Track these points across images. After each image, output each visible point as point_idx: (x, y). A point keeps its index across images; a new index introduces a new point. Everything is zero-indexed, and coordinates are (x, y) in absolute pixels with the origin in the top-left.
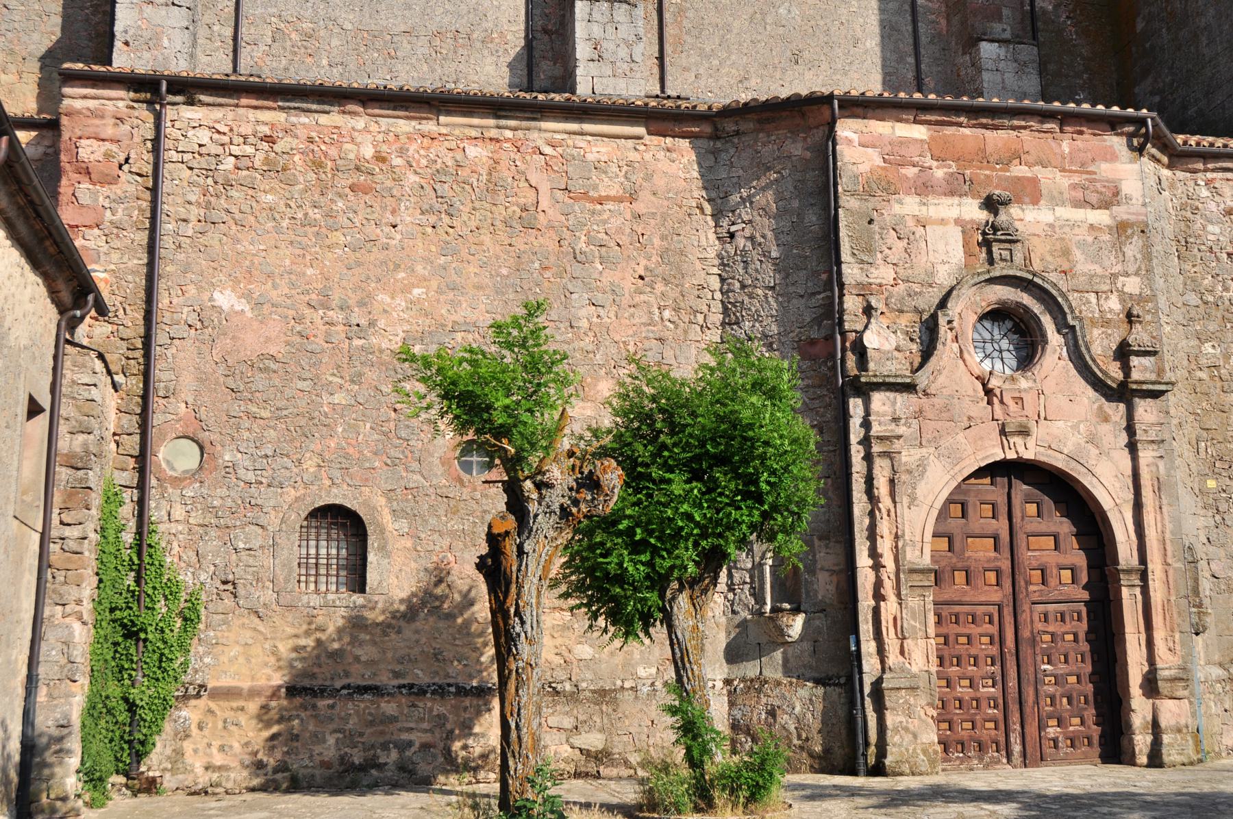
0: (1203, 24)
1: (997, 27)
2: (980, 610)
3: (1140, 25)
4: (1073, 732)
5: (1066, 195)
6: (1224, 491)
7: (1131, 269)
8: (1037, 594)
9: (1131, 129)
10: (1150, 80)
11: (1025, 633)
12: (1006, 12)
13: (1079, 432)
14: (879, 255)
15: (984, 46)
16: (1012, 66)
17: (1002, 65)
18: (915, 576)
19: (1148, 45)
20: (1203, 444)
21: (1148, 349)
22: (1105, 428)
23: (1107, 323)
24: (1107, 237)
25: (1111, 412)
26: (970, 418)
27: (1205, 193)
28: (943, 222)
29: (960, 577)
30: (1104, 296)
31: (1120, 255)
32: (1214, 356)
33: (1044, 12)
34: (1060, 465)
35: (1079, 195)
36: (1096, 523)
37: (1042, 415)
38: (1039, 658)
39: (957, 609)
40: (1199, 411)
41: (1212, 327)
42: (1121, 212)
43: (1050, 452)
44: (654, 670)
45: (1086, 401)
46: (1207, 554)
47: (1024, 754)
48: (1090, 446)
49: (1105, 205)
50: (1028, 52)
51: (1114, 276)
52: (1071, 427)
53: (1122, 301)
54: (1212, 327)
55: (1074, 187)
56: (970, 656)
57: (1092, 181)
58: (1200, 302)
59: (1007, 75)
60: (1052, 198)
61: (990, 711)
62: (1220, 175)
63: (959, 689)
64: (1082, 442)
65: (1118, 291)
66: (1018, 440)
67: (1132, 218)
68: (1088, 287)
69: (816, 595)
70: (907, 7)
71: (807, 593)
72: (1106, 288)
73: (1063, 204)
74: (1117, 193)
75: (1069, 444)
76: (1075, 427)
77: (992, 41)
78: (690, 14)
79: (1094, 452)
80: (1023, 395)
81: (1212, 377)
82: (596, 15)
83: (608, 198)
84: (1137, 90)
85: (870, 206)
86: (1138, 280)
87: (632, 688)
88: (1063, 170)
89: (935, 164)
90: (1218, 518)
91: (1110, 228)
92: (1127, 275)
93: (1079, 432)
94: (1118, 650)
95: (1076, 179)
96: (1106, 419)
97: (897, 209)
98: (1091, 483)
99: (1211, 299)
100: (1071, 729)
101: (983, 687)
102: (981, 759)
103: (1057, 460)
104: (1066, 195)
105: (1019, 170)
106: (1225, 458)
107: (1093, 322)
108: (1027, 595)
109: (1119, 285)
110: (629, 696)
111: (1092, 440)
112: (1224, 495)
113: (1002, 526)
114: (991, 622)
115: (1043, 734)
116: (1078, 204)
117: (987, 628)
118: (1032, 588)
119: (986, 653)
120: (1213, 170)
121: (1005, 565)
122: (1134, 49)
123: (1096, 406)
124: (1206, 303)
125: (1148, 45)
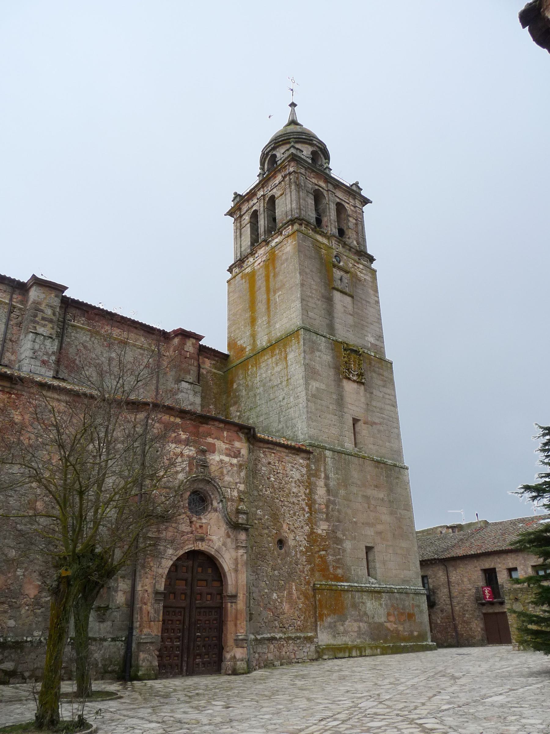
0: (258, 392)
1: (188, 377)
2: (178, 610)
3: (235, 386)
5: (224, 452)
9: (246, 431)
10: (237, 406)
11: (193, 620)
12: (192, 372)
15: (183, 383)
16: (192, 392)
17: (189, 391)
19: (237, 394)
22: (229, 540)
23: (233, 500)
24: (235, 469)
25: (231, 534)
29: (172, 596)
32: (260, 515)
33: (203, 374)
34: (213, 553)
35: (228, 452)
36: (221, 577)
39: (170, 609)
43: (209, 548)
44: (40, 633)
47: (187, 671)
48: (223, 547)
50: (198, 388)
51: (237, 483)
53: (238, 493)
54: (261, 504)
55: (227, 449)
56: (172, 629)
57: (232, 447)
59: (190, 396)
60: (219, 452)
62: (267, 450)
63: (167, 643)
64: (221, 545)
68: (228, 486)
69: (116, 601)
71: (113, 600)
72: (233, 487)
73: (223, 455)
74: (240, 453)
75: (216, 545)
76: (219, 539)
77: (186, 382)
79: (224, 549)
80: (203, 525)
81: (259, 523)
82: (37, 340)
84: (231, 409)
86: (243, 485)
87: (30, 641)
88: (224, 442)
89: (182, 433)
92: (240, 483)
94: (224, 628)
95: (227, 446)
96: (229, 536)
99: (261, 494)
100: (205, 660)
104: (224, 452)
105: (210, 440)
110: (29, 645)
111: (224, 544)
113: (189, 576)
114: (181, 615)
116: (227, 455)
117: (179, 617)
118: (197, 602)
121: (188, 592)
122: (232, 394)
124: (260, 495)
125: (237, 394)
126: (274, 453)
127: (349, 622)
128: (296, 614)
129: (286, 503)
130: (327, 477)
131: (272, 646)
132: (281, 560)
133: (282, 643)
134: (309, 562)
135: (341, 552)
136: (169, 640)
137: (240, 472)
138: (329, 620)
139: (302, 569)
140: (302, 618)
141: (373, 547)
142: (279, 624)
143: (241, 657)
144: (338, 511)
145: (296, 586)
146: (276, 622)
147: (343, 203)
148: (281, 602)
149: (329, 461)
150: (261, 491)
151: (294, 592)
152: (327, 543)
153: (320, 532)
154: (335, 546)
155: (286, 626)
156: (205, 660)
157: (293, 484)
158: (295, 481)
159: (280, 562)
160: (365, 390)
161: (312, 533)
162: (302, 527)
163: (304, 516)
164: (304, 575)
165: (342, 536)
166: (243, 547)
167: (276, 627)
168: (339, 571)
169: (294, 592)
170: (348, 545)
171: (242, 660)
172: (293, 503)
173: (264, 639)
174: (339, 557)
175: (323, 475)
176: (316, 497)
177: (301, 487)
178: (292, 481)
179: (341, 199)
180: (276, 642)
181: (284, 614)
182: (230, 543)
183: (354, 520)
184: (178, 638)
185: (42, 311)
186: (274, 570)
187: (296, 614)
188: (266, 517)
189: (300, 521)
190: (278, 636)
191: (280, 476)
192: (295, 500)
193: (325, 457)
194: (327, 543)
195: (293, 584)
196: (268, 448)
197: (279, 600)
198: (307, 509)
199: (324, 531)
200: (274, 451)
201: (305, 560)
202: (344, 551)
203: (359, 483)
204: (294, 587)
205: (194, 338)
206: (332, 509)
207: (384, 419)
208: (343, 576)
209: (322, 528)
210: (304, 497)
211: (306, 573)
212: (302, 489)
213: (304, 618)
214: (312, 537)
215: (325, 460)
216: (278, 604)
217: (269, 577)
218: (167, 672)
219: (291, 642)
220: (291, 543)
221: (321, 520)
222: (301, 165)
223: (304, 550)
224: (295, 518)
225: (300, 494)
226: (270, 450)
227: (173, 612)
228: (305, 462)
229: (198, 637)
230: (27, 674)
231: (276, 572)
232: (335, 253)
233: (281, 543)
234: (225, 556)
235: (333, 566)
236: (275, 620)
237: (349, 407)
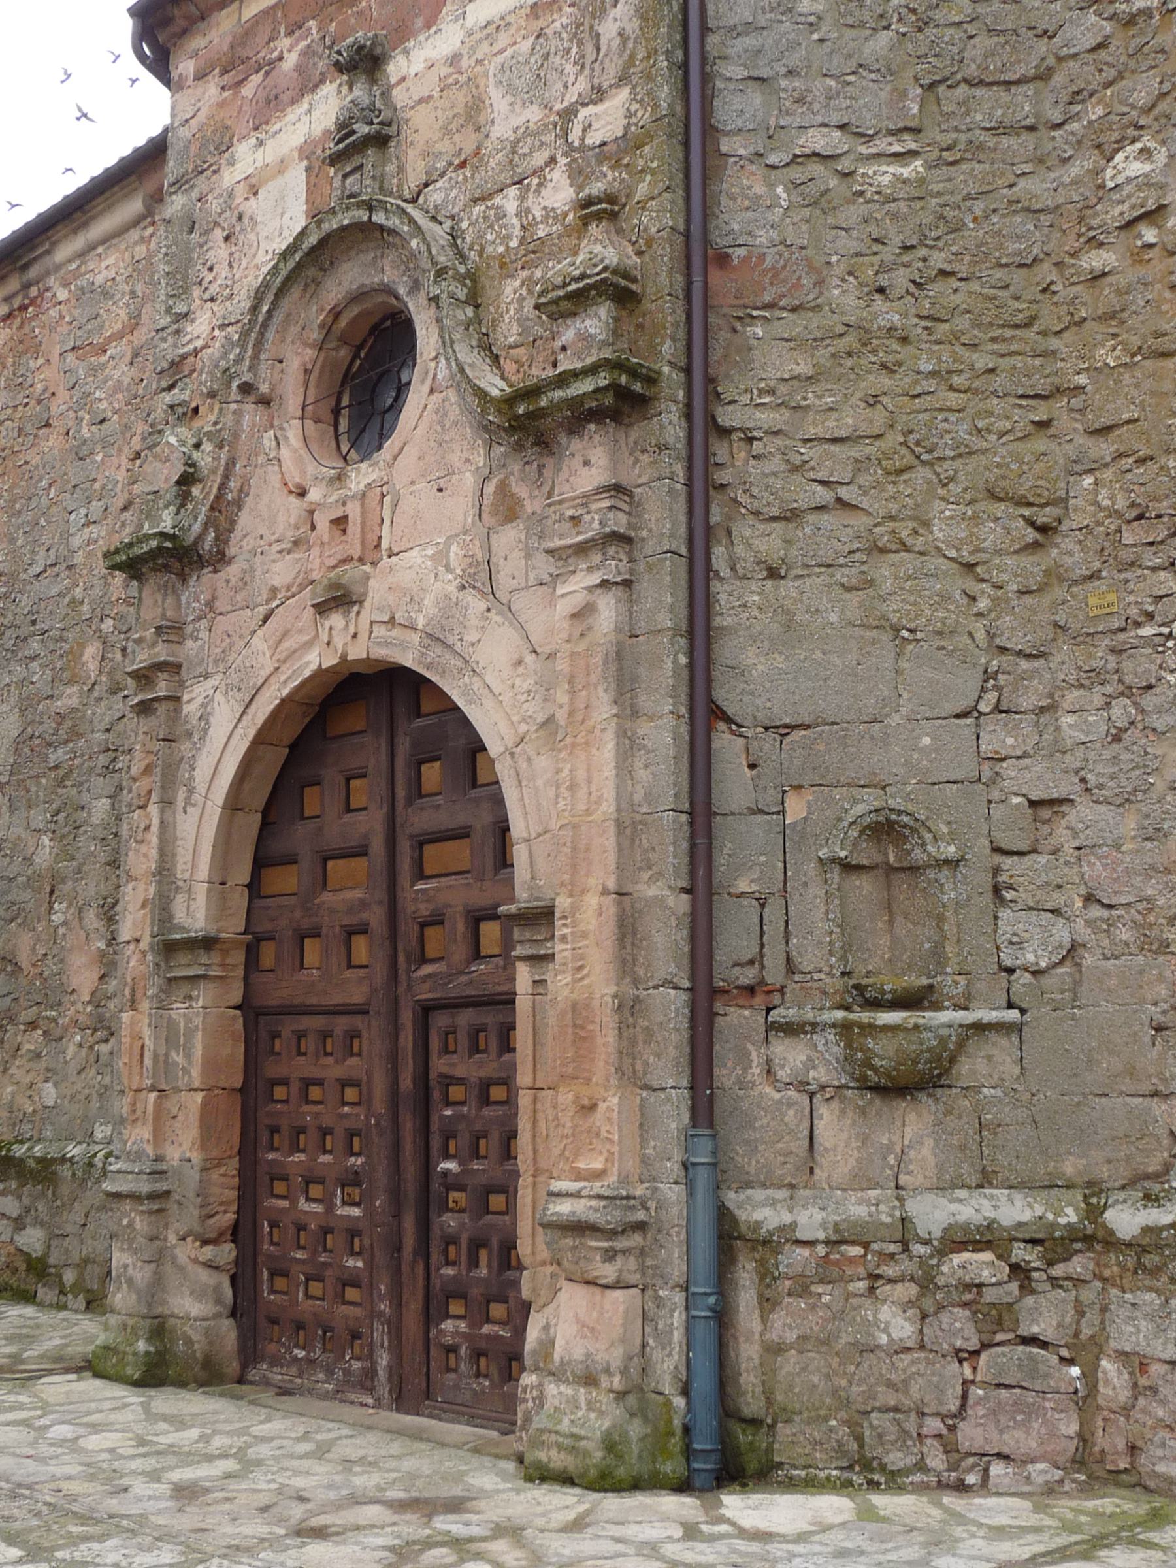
4: (488, 1337)
6: (1150, 616)
7: (612, 69)
8: (426, 986)
13: (448, 569)
14: (196, 292)
18: (183, 958)
21: (573, 287)
22: (508, 538)
25: (521, 490)
26: (274, 590)
28: (282, 167)
30: (536, 181)
31: (589, 49)
37: (385, 545)
38: (436, 1142)
40: (1082, 380)
43: (396, 632)
45: (469, 480)
46: (1075, 834)
51: (569, 114)
52: (432, 558)
53: (577, 174)
58: (1108, 27)
61: (350, 1263)
63: (303, 1204)
64: (452, 588)
65: (570, 149)
66: (336, 620)
76: (441, 558)
79: (476, 604)
83: (110, 339)
85: (195, 194)
86: (624, 93)
90: (1121, 711)
92: (598, 94)
93: (448, 569)
97: (230, 177)
98: (466, 691)
101: (344, 1203)
102: (330, 1372)
103: (403, 646)
106: (1154, 509)
107: (505, 266)
108: (410, 988)
109: (574, 136)
112: (1147, 631)
115: (433, 1333)
119: (346, 1124)
121: (376, 917)
123: (490, 488)
136: (316, 1191)
143: (578, 1354)
156: (486, 1329)
166: (582, 549)
171: (589, 1380)
182: (517, 555)
184: (352, 1180)
218: (311, 1362)
227: (325, 1035)
229: (451, 1183)
230: (69, 1277)
234: (481, 656)
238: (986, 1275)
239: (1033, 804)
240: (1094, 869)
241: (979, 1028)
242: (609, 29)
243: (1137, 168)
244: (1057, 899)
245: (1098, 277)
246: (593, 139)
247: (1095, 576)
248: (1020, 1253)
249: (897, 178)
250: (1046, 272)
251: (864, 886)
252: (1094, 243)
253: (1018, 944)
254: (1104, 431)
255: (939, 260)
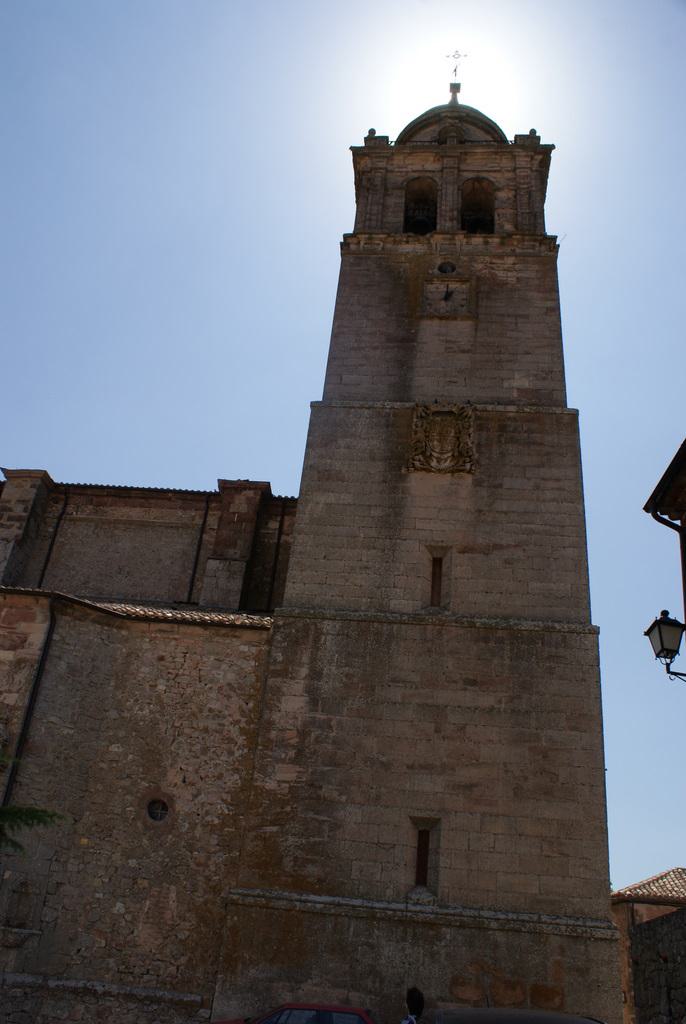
7: (15, 688)
12: (240, 542)
20: (88, 813)
27: (146, 646)
40: (92, 790)
41: (121, 733)
42: (22, 653)
49: (13, 648)
67: (28, 656)
70: (196, 542)
78: (67, 547)
86: (16, 695)
90: (82, 866)
91: (11, 662)
92: (10, 691)
112: (91, 850)
120: (156, 631)
126: (175, 639)
127: (315, 985)
128: (167, 951)
129: (187, 731)
130: (315, 674)
131: (81, 1008)
132: (150, 839)
133: (108, 1004)
134: (225, 845)
135: (326, 827)
137: (16, 673)
138: (252, 972)
139: (202, 860)
140: (183, 960)
141: (439, 819)
142: (117, 965)
144: (334, 742)
145: (178, 893)
146: (111, 961)
147: (484, 175)
148: (134, 920)
149: (329, 643)
150: (130, 710)
151: (172, 904)
152: (288, 809)
153: (271, 785)
154: (311, 815)
155: (137, 970)
157: (213, 695)
158: (220, 688)
159: (145, 841)
160: (477, 483)
161: (247, 785)
162: (220, 777)
163: (231, 753)
164: (207, 873)
165: (335, 794)
167: (108, 970)
168: (312, 870)
169: (172, 904)
170: (352, 816)
172: (206, 730)
173: (65, 989)
174: (317, 839)
175: (304, 671)
176: (276, 716)
177: (235, 699)
178: (211, 688)
179: (478, 171)
180: (93, 1000)
181: (136, 946)
183: (384, 759)
185: (10, 510)
186: (128, 858)
187: (167, 951)
188: (131, 756)
189: (216, 765)
190: (100, 989)
191: (184, 680)
192: (212, 724)
193: (319, 633)
194: (288, 809)
195: (173, 887)
196: (161, 631)
197: (128, 917)
198: (241, 740)
199: (284, 785)
200: (176, 636)
201: (216, 842)
202: (336, 826)
203: (416, 678)
204: (173, 895)
205: (250, 489)
206: (317, 738)
207: (533, 532)
208: (320, 881)
209: (281, 776)
210: (237, 717)
211: (213, 868)
212: (236, 702)
213: (190, 960)
214: (245, 798)
215: (317, 640)
216: (124, 923)
217: (111, 870)
219: (132, 1006)
220: (182, 806)
221: (283, 761)
222: (376, 157)
223: (216, 821)
224: (203, 758)
225: (226, 713)
226: (165, 635)
228: (254, 650)
231: (132, 863)
232: (439, 261)
233: (158, 806)
235: (296, 859)
236: (110, 956)
237: (419, 525)
238: (18, 995)
239: (57, 883)
240: (66, 901)
241: (34, 934)
242: (18, 678)
243: (116, 750)
244: (56, 906)
245: (102, 769)
246: (6, 702)
247: (83, 835)
248: (28, 990)
249: (68, 734)
250: (91, 763)
251: (16, 896)
252: (103, 761)
253: (45, 916)
254: (93, 803)
255: (72, 754)
